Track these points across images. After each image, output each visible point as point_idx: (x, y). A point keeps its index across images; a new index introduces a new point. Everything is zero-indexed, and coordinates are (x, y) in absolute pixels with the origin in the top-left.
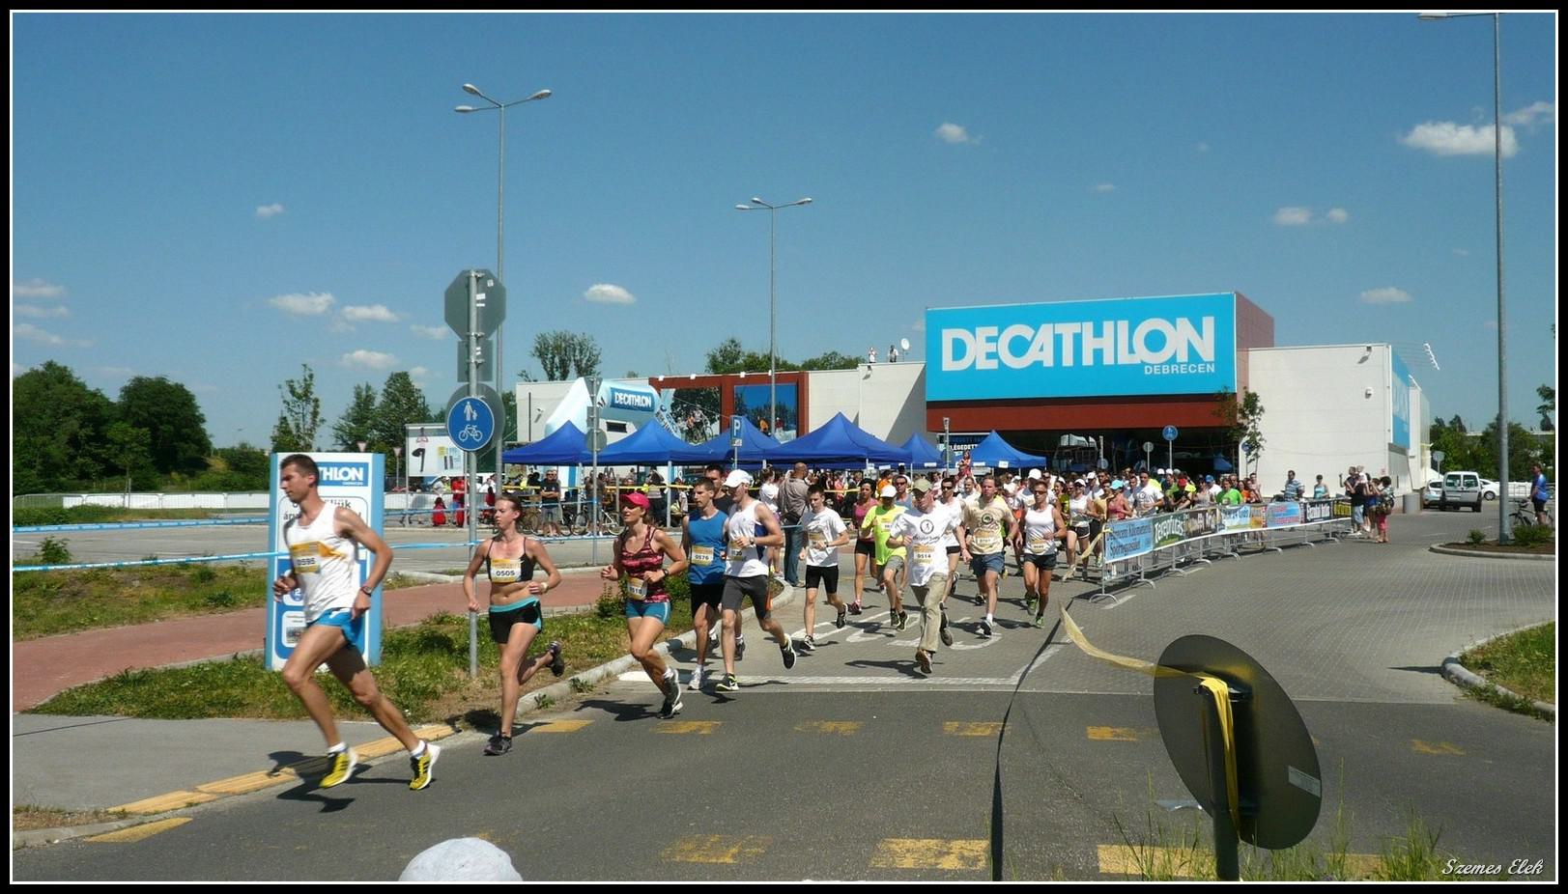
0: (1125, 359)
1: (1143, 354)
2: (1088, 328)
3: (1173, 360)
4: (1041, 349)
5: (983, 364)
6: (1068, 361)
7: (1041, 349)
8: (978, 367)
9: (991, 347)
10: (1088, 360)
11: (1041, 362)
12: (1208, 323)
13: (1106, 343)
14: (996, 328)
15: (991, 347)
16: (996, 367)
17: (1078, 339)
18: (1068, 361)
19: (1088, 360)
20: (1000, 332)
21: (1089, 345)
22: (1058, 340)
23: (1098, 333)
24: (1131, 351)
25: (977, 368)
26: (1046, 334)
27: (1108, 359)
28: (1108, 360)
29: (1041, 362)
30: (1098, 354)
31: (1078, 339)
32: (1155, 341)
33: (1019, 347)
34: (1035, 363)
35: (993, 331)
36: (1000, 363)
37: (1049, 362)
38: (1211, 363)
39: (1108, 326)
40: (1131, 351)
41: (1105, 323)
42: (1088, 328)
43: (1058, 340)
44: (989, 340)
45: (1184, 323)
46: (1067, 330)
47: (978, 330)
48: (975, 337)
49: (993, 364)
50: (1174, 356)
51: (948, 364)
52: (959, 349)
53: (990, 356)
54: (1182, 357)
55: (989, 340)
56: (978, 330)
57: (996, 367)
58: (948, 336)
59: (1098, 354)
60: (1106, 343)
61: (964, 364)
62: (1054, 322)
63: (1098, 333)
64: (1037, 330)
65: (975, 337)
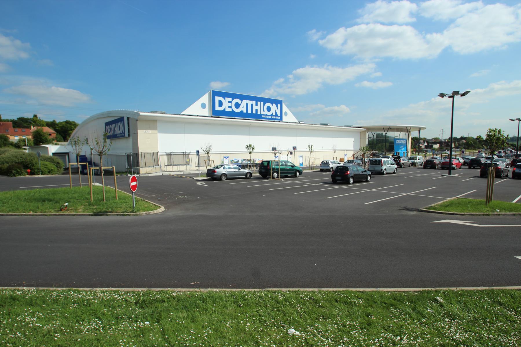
0: (262, 113)
1: (266, 112)
2: (254, 103)
3: (272, 115)
4: (243, 107)
5: (228, 110)
6: (249, 112)
7: (243, 107)
8: (226, 110)
9: (230, 105)
10: (254, 112)
11: (243, 111)
12: (279, 105)
13: (258, 108)
14: (231, 99)
15: (230, 105)
16: (231, 111)
17: (252, 105)
18: (249, 112)
19: (254, 112)
20: (232, 101)
21: (255, 108)
22: (247, 105)
23: (257, 105)
24: (264, 111)
25: (226, 110)
26: (244, 102)
27: (259, 113)
28: (259, 113)
29: (243, 111)
30: (257, 110)
31: (252, 105)
32: (269, 109)
33: (237, 105)
34: (242, 111)
35: (230, 99)
36: (232, 110)
37: (245, 111)
38: (279, 116)
39: (259, 103)
40: (264, 111)
41: (258, 102)
42: (254, 103)
43: (247, 105)
44: (229, 102)
45: (274, 105)
46: (250, 102)
47: (226, 98)
48: (225, 100)
49: (230, 110)
50: (272, 114)
51: (217, 108)
52: (221, 104)
53: (230, 107)
54: (274, 114)
55: (229, 102)
56: (226, 98)
57: (231, 111)
58: (217, 99)
59: (257, 110)
60: (258, 108)
61: (221, 109)
62: (246, 99)
63: (257, 105)
64: (242, 101)
65: (225, 100)
